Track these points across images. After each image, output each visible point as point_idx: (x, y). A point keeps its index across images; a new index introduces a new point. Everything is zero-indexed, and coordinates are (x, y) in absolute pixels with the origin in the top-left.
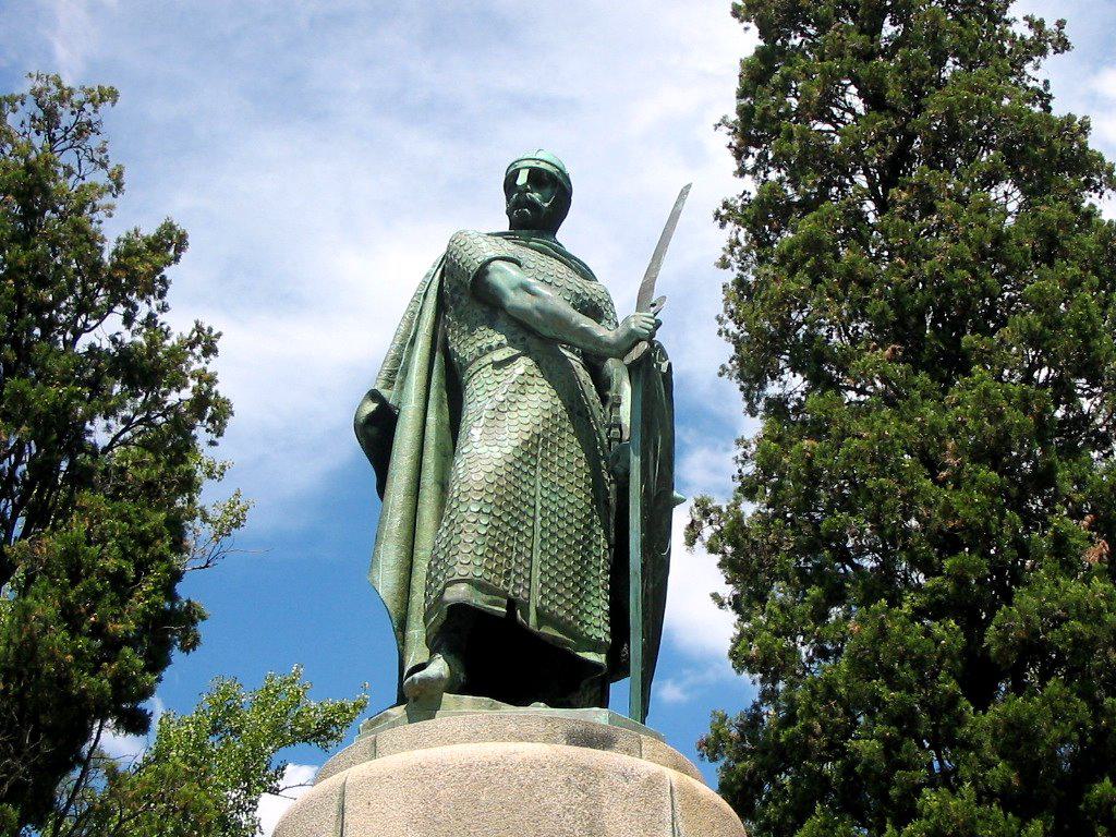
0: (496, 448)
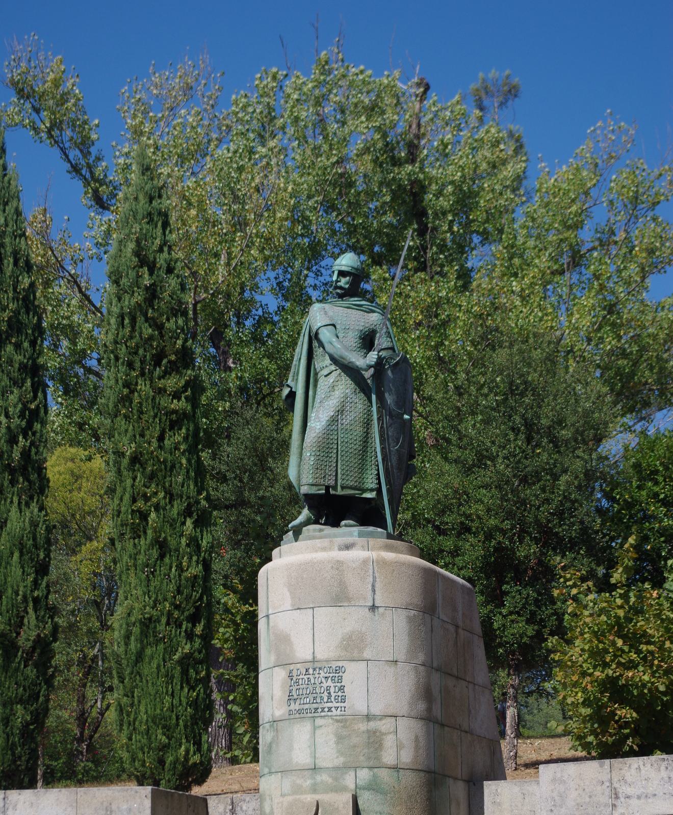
0: (318, 424)
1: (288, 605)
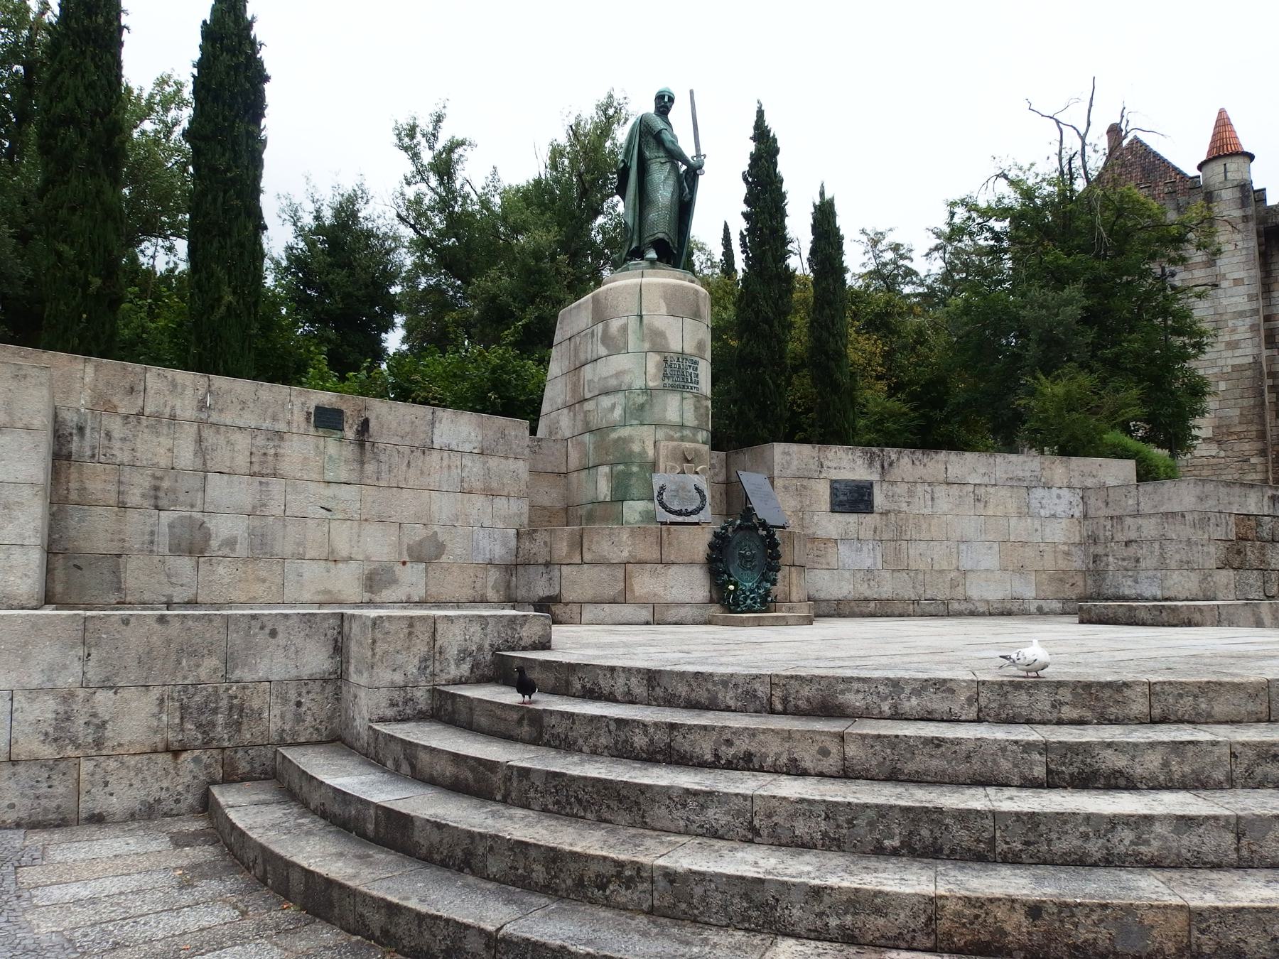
1: (664, 310)
